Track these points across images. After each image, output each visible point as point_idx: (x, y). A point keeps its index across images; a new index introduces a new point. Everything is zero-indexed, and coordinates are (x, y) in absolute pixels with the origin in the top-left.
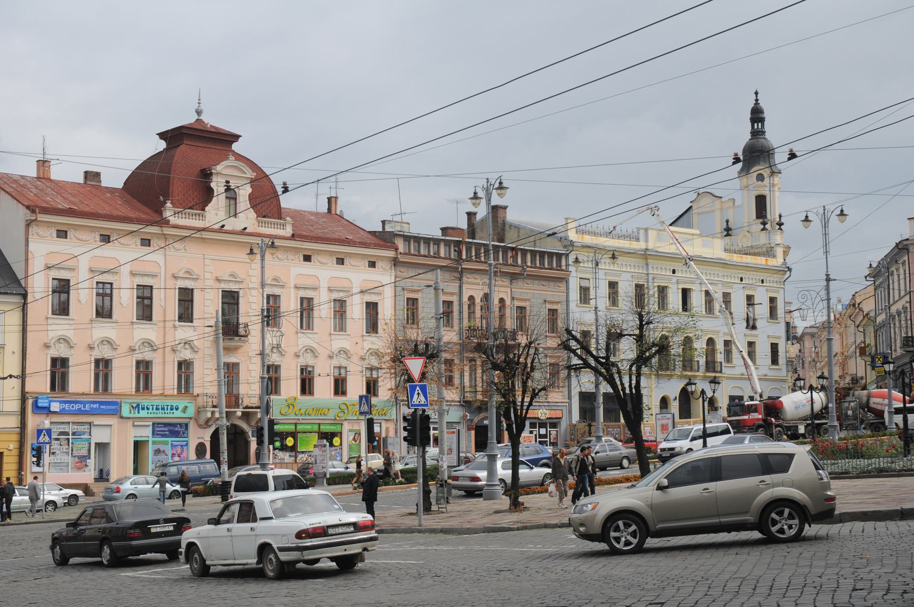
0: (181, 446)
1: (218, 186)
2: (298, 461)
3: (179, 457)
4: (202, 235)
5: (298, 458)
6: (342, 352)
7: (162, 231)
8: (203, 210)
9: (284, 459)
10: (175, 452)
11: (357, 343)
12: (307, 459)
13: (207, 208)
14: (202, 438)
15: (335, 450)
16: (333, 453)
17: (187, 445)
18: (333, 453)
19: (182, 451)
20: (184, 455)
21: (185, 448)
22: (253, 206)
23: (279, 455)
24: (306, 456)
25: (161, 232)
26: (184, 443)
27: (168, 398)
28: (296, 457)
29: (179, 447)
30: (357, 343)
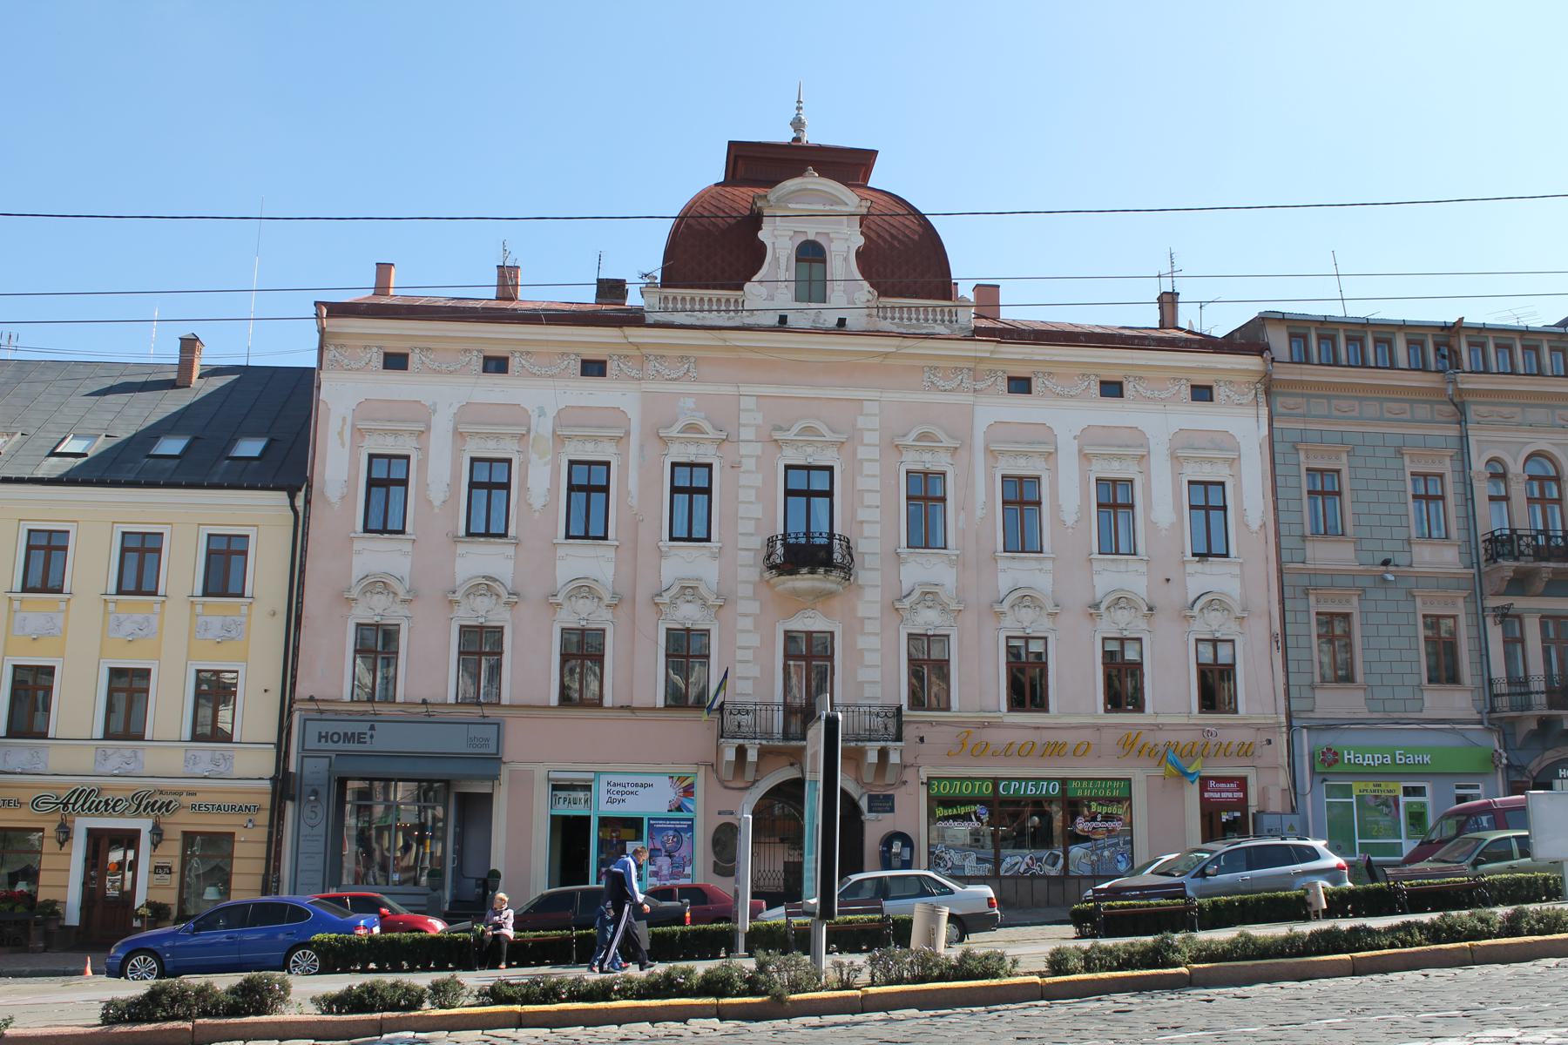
0: (676, 830)
1: (776, 237)
2: (1002, 873)
3: (670, 856)
4: (725, 340)
5: (1004, 866)
6: (1123, 603)
7: (625, 337)
8: (740, 288)
9: (963, 867)
10: (658, 846)
11: (1168, 580)
12: (1029, 868)
13: (747, 286)
14: (732, 813)
15: (1110, 846)
16: (1106, 853)
17: (691, 828)
18: (1106, 853)
19: (679, 843)
20: (684, 851)
21: (686, 837)
22: (866, 272)
23: (948, 857)
24: (1027, 859)
25: (625, 341)
26: (684, 825)
27: (640, 714)
28: (997, 862)
29: (671, 833)
30: (1168, 580)
